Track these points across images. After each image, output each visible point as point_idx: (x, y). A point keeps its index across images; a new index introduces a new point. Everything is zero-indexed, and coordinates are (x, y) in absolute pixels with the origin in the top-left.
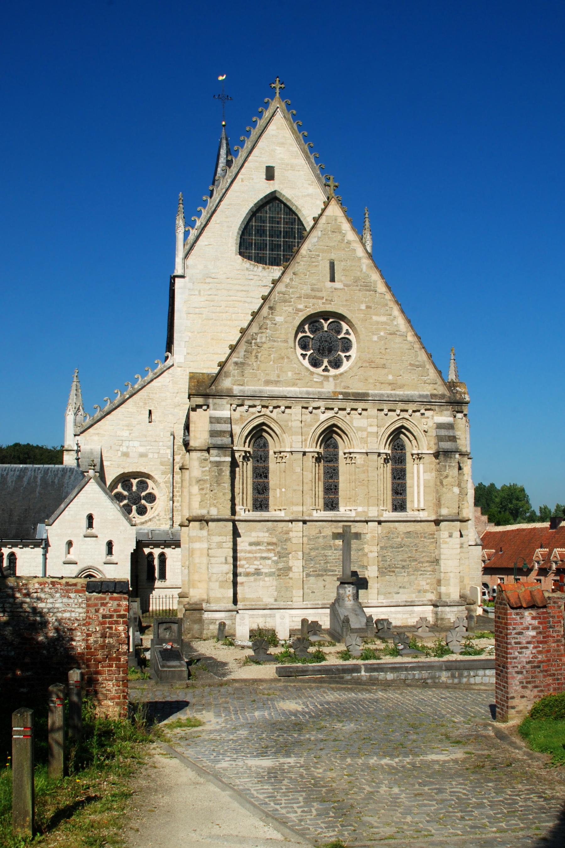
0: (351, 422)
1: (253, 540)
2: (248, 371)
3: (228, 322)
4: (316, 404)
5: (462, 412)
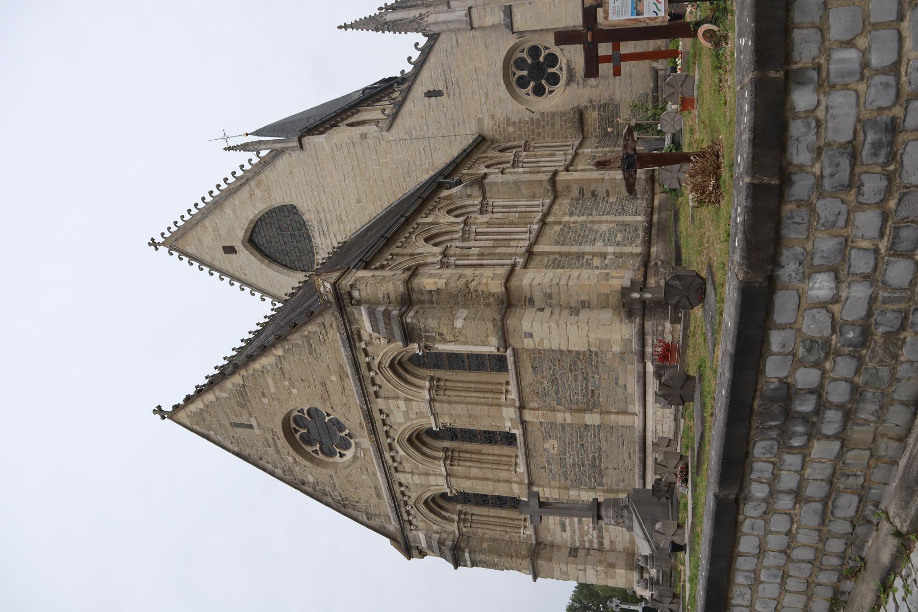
0: (400, 424)
1: (558, 528)
2: (372, 510)
4: (390, 461)
5: (350, 293)
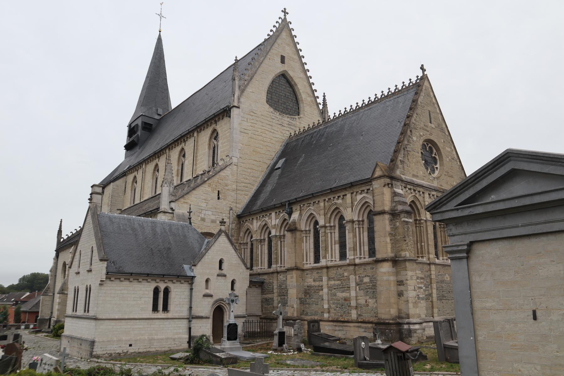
3: (262, 142)
